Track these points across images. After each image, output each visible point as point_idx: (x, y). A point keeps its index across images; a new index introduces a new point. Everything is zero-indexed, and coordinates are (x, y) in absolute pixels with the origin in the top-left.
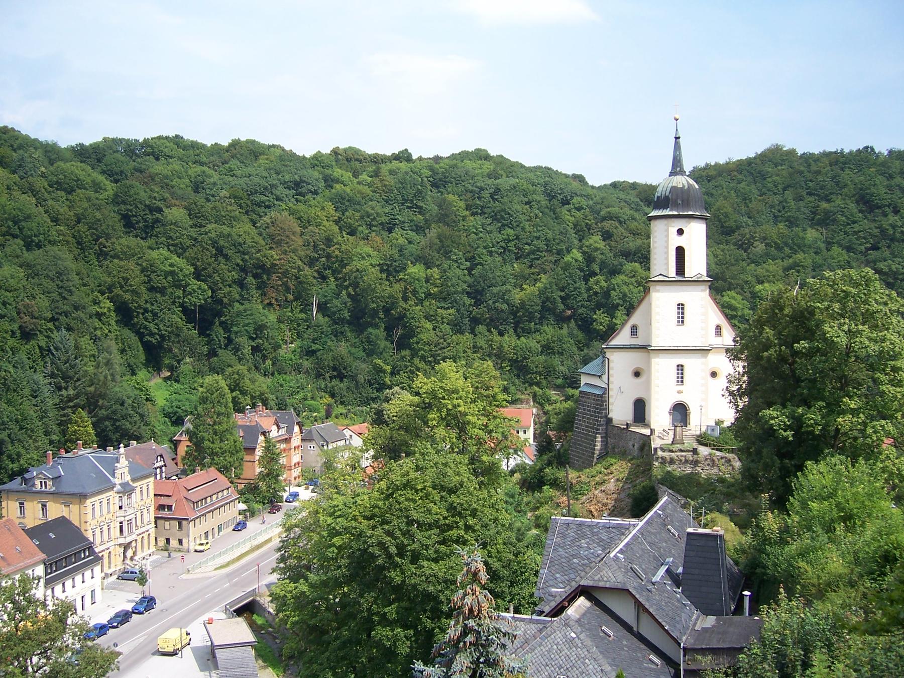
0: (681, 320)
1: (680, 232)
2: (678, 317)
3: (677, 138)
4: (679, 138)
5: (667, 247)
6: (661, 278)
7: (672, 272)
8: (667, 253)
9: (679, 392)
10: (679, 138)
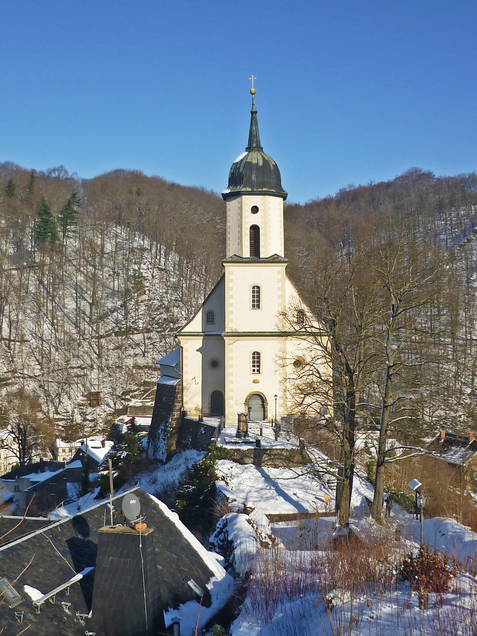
0: (256, 304)
1: (255, 210)
2: (253, 301)
3: (253, 113)
4: (256, 112)
5: (240, 226)
6: (235, 259)
7: (246, 253)
8: (240, 232)
9: (255, 382)
10: (256, 112)
